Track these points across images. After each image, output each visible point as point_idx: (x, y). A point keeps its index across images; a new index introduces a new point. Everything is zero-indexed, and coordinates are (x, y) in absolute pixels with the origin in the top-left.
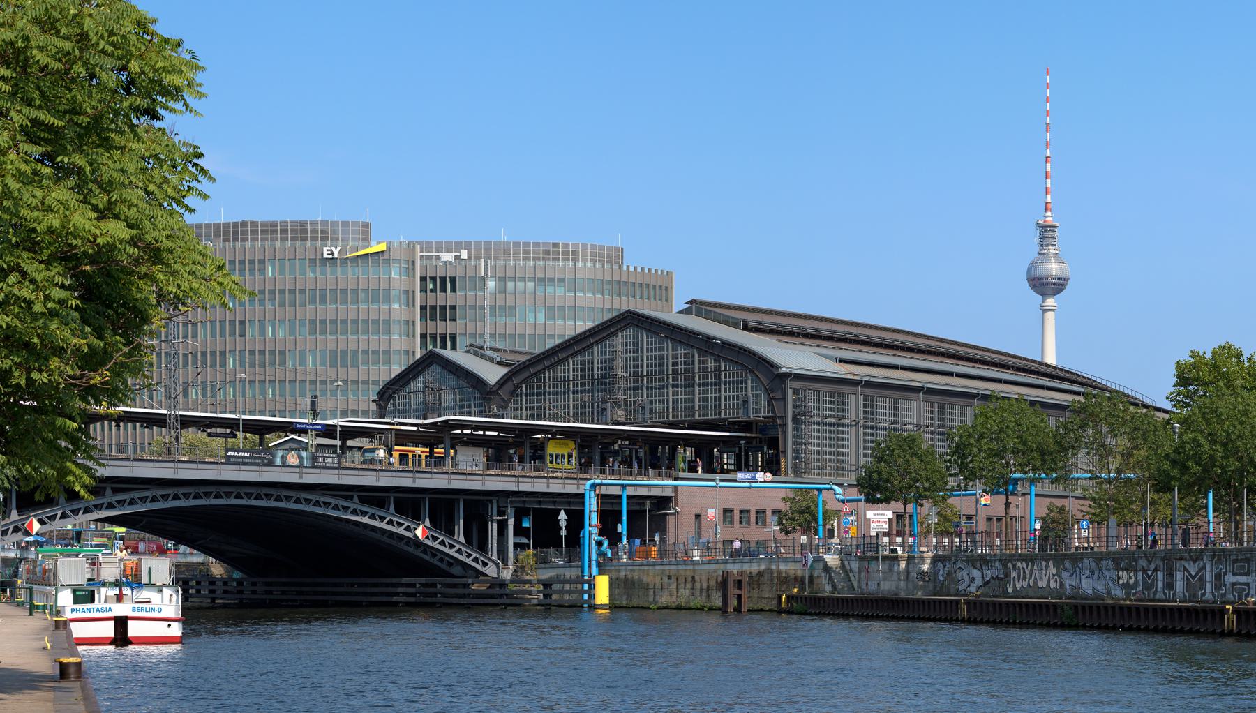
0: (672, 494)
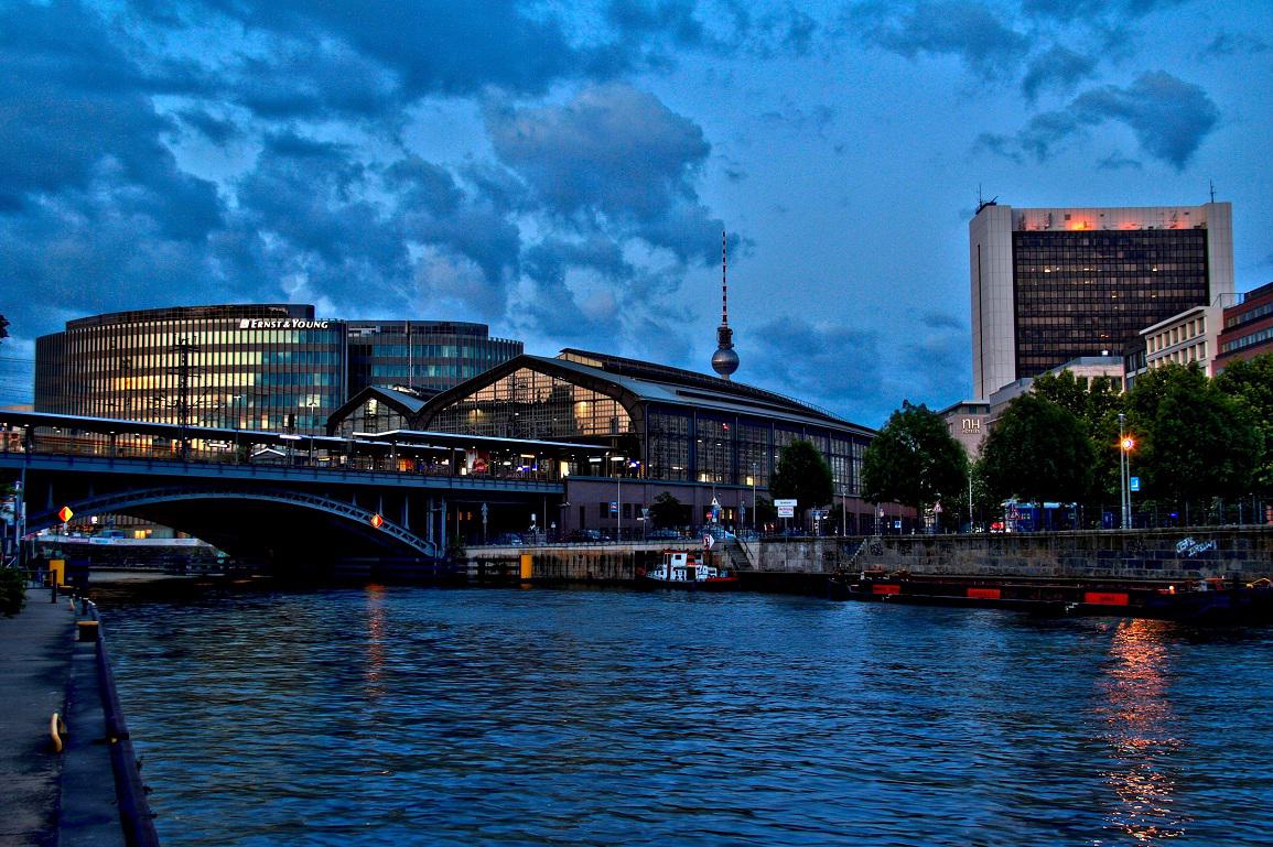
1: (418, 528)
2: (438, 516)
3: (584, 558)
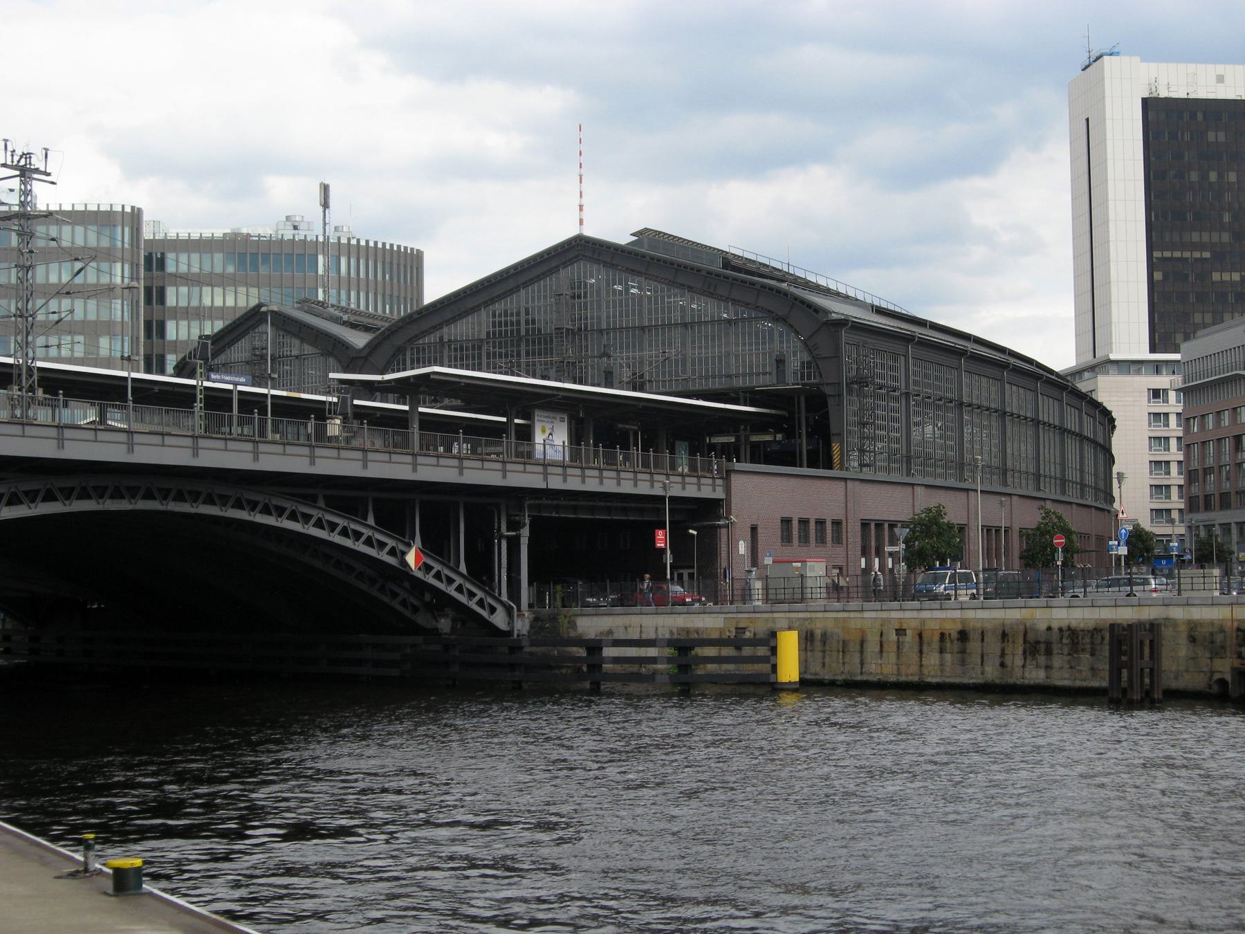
0: (719, 494)
1: (481, 571)
2: (514, 544)
3: (910, 638)
